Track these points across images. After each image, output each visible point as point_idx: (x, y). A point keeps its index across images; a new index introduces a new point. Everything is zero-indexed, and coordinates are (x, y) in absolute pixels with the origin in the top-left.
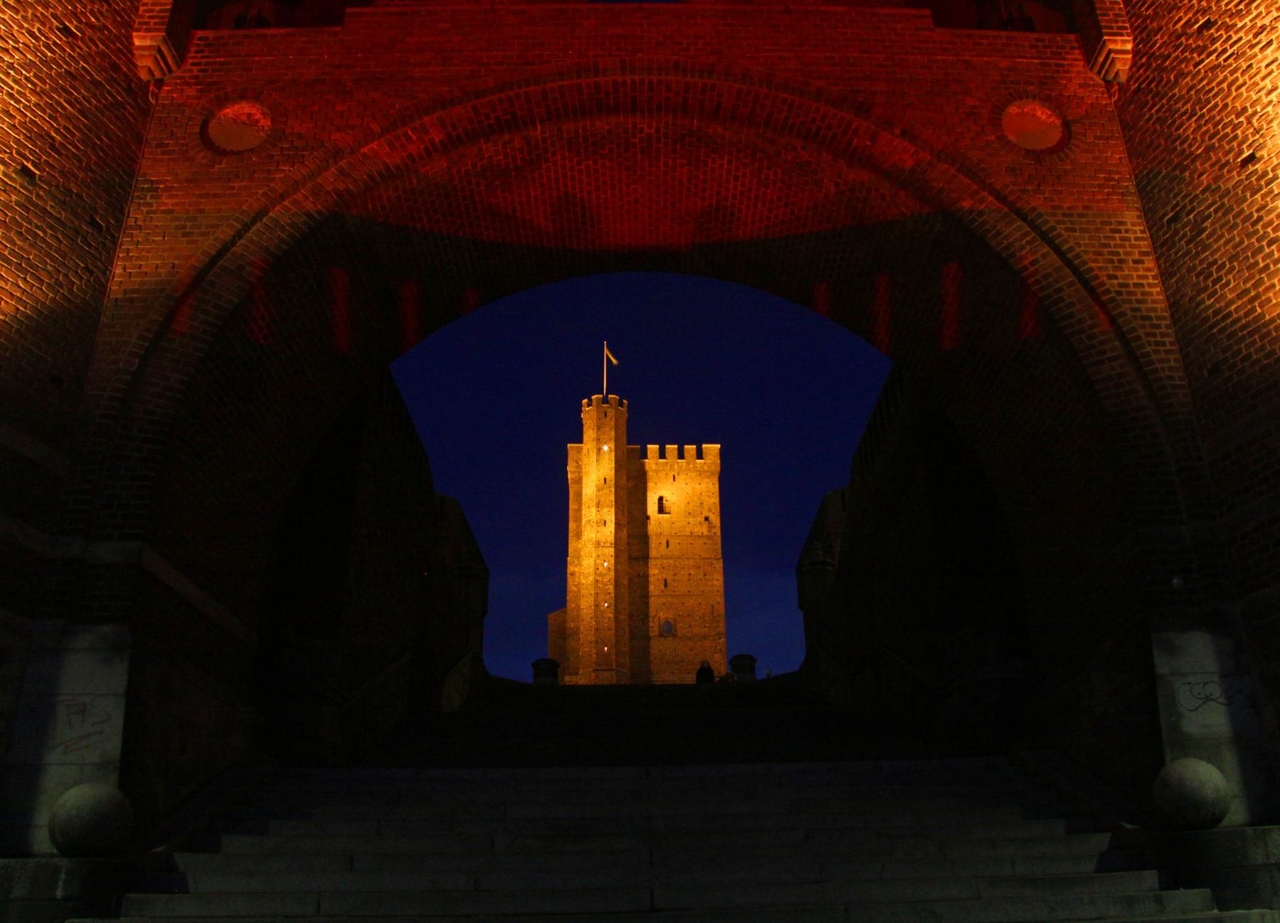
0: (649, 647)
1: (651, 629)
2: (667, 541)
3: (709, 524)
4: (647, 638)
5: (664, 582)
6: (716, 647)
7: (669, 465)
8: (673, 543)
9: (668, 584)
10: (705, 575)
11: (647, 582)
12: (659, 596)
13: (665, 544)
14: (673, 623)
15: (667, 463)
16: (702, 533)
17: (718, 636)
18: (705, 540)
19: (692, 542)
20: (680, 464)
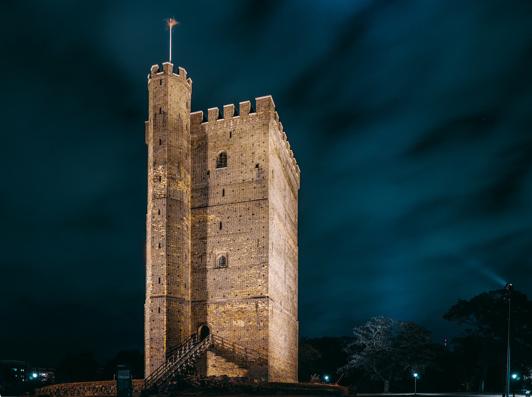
0: (206, 278)
1: (208, 263)
2: (224, 190)
3: (258, 170)
4: (205, 270)
5: (219, 225)
6: (259, 274)
7: (225, 123)
8: (228, 190)
9: (223, 226)
10: (253, 215)
11: (206, 226)
12: (215, 236)
13: (222, 193)
14: (226, 257)
15: (224, 122)
16: (253, 179)
17: (262, 265)
18: (255, 185)
19: (244, 188)
20: (235, 120)
